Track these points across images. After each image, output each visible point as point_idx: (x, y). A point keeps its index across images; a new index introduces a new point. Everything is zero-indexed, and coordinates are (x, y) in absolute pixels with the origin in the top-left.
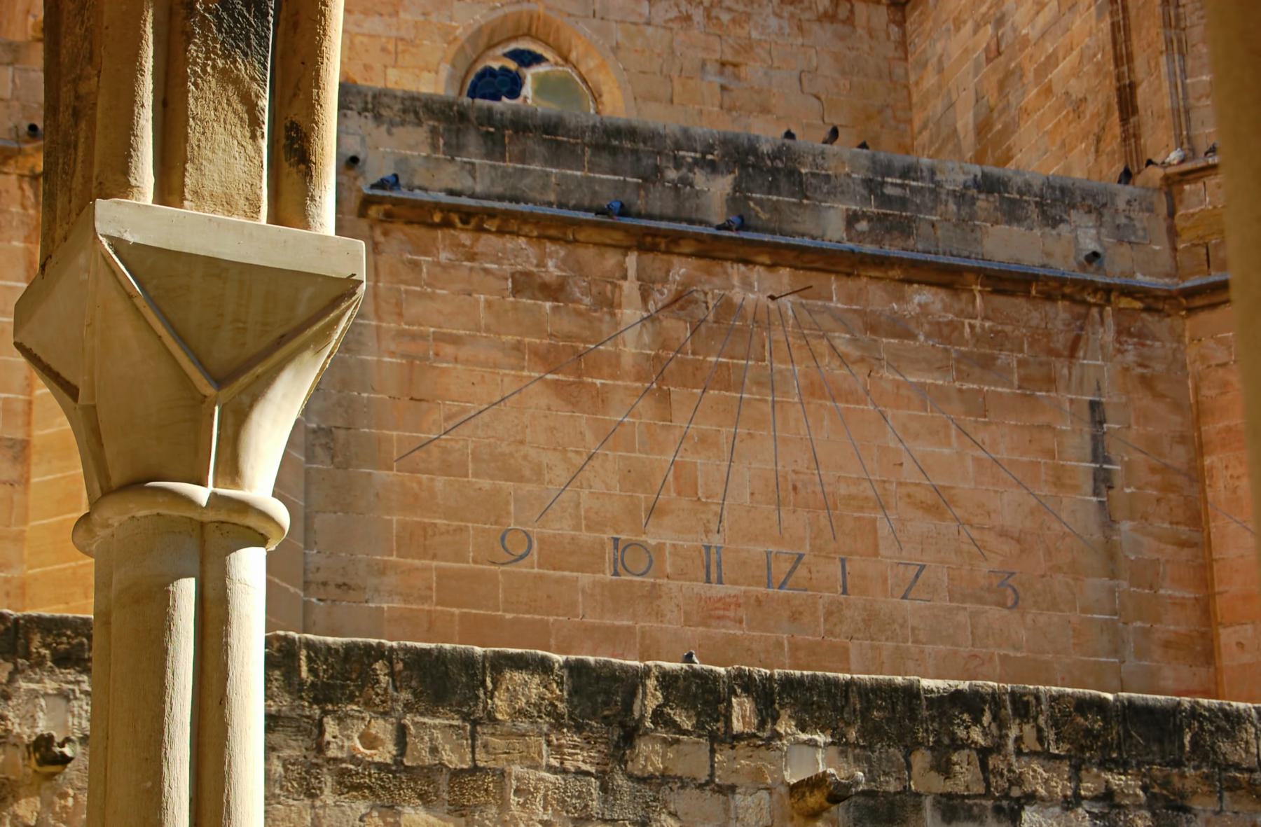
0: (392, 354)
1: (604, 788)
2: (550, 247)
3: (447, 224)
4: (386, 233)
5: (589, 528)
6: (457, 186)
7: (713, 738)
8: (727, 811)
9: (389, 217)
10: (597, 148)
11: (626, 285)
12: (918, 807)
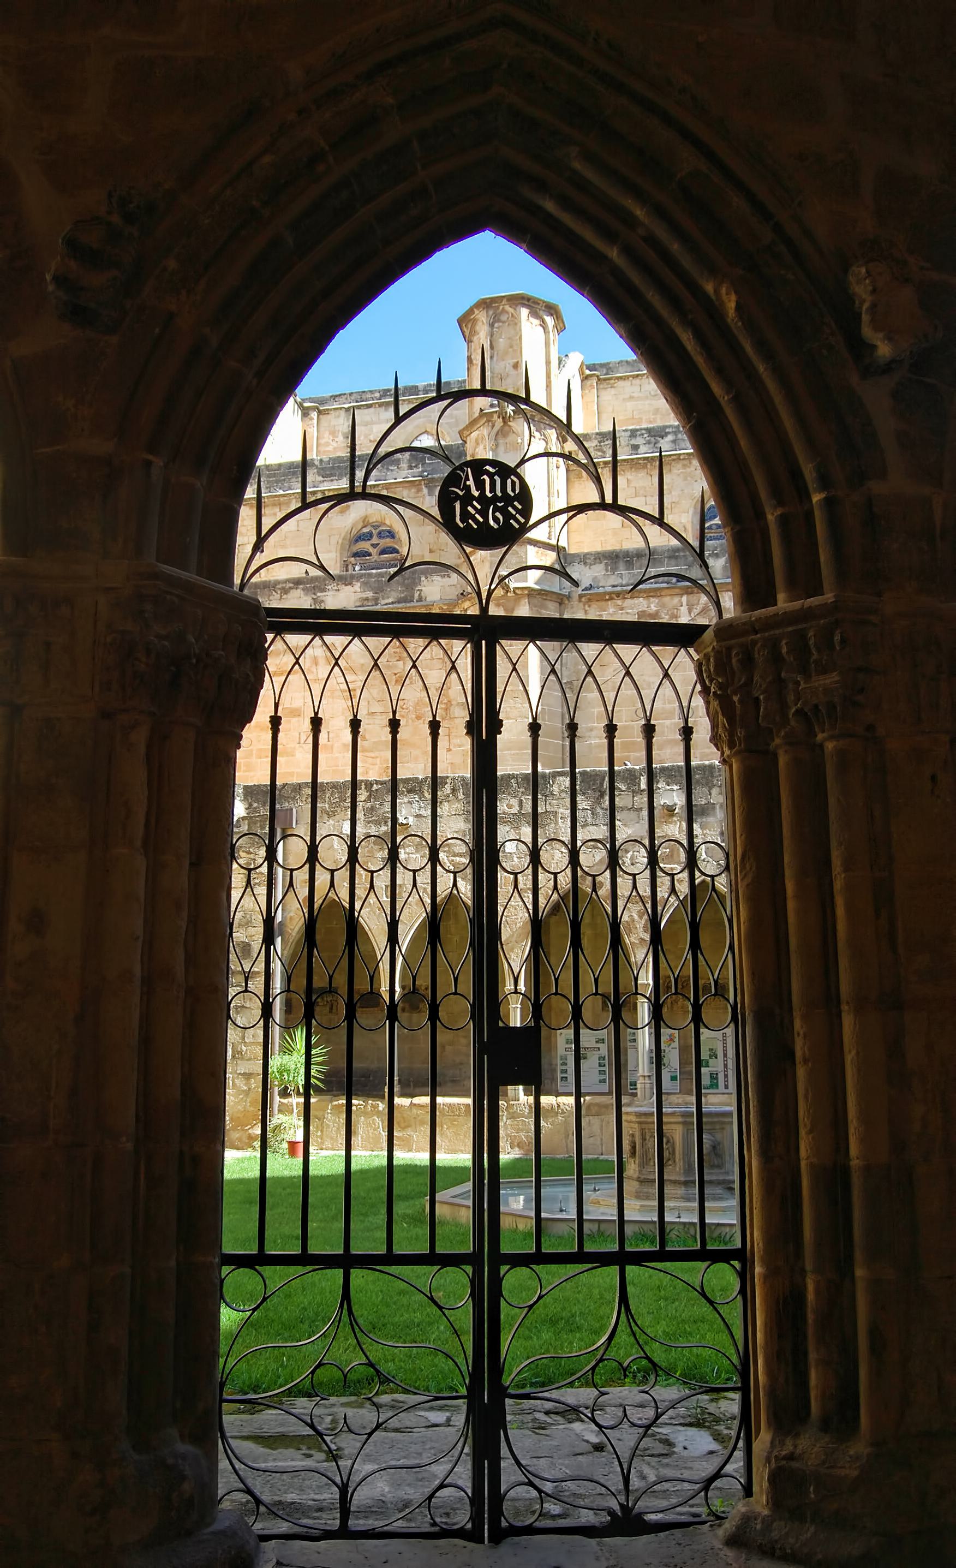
0: (593, 650)
1: (593, 814)
2: (652, 599)
3: (611, 599)
4: (589, 606)
5: (669, 703)
6: (616, 583)
7: (633, 792)
8: (639, 817)
9: (590, 600)
10: (670, 557)
11: (682, 608)
12: (714, 808)
